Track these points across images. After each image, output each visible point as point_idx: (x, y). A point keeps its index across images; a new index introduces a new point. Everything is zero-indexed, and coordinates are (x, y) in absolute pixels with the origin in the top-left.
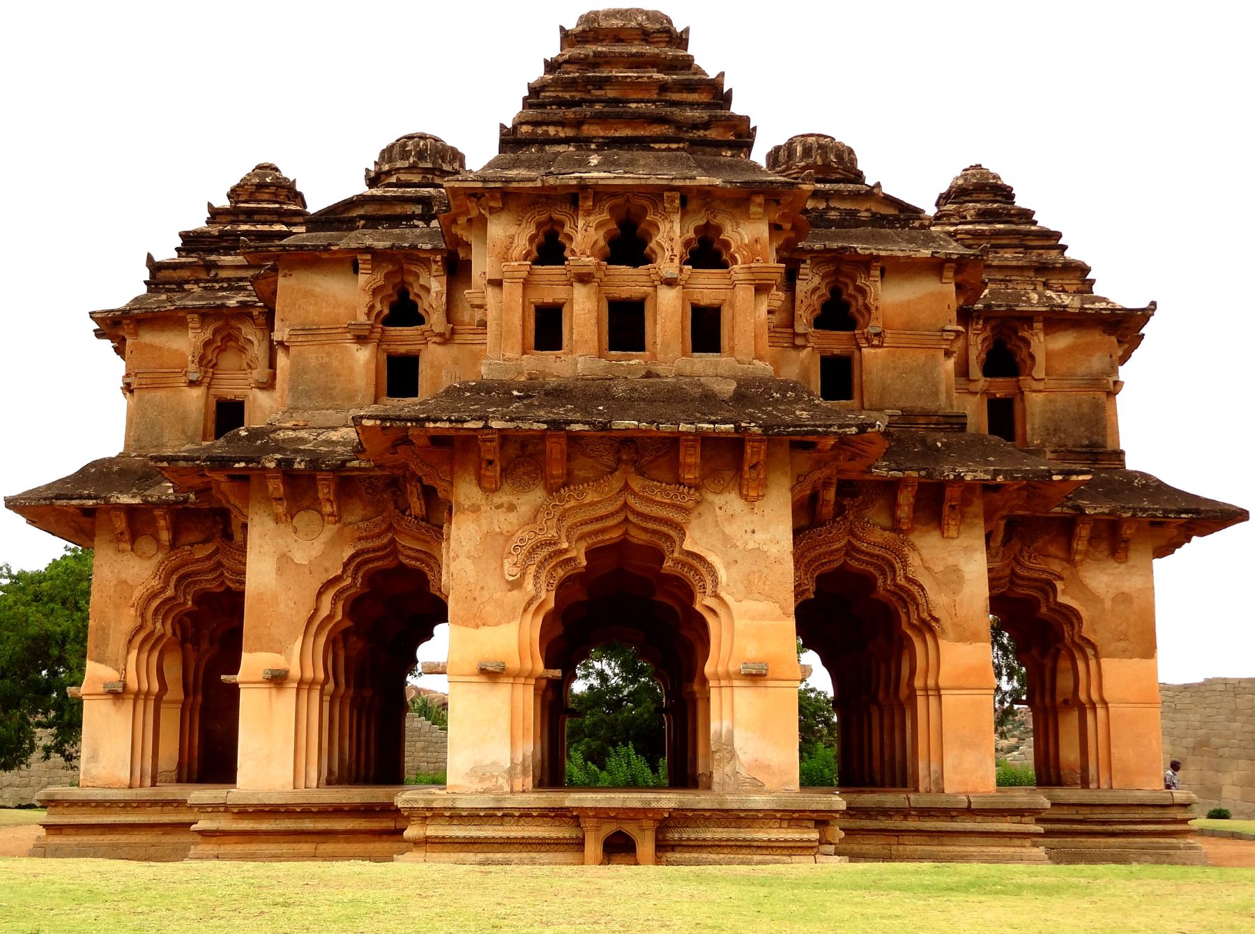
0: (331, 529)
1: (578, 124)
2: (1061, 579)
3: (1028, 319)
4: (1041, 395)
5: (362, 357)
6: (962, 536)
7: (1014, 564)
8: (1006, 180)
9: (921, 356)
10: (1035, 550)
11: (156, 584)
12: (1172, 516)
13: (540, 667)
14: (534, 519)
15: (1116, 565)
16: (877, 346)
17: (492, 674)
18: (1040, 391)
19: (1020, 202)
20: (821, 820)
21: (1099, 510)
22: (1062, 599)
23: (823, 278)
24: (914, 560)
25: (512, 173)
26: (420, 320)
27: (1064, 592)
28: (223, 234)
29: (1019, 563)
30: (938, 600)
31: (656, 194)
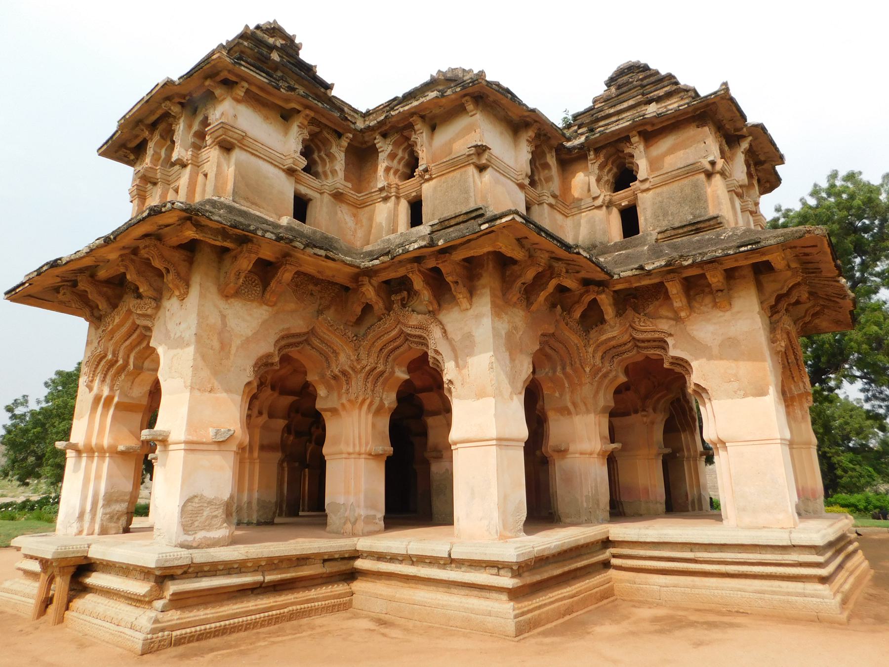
2: (670, 335)
3: (623, 138)
4: (651, 192)
6: (474, 307)
7: (631, 330)
8: (643, 61)
9: (457, 174)
10: (645, 315)
12: (731, 252)
15: (721, 314)
16: (431, 179)
18: (648, 190)
21: (657, 264)
22: (673, 352)
23: (396, 144)
27: (674, 346)
29: (634, 329)
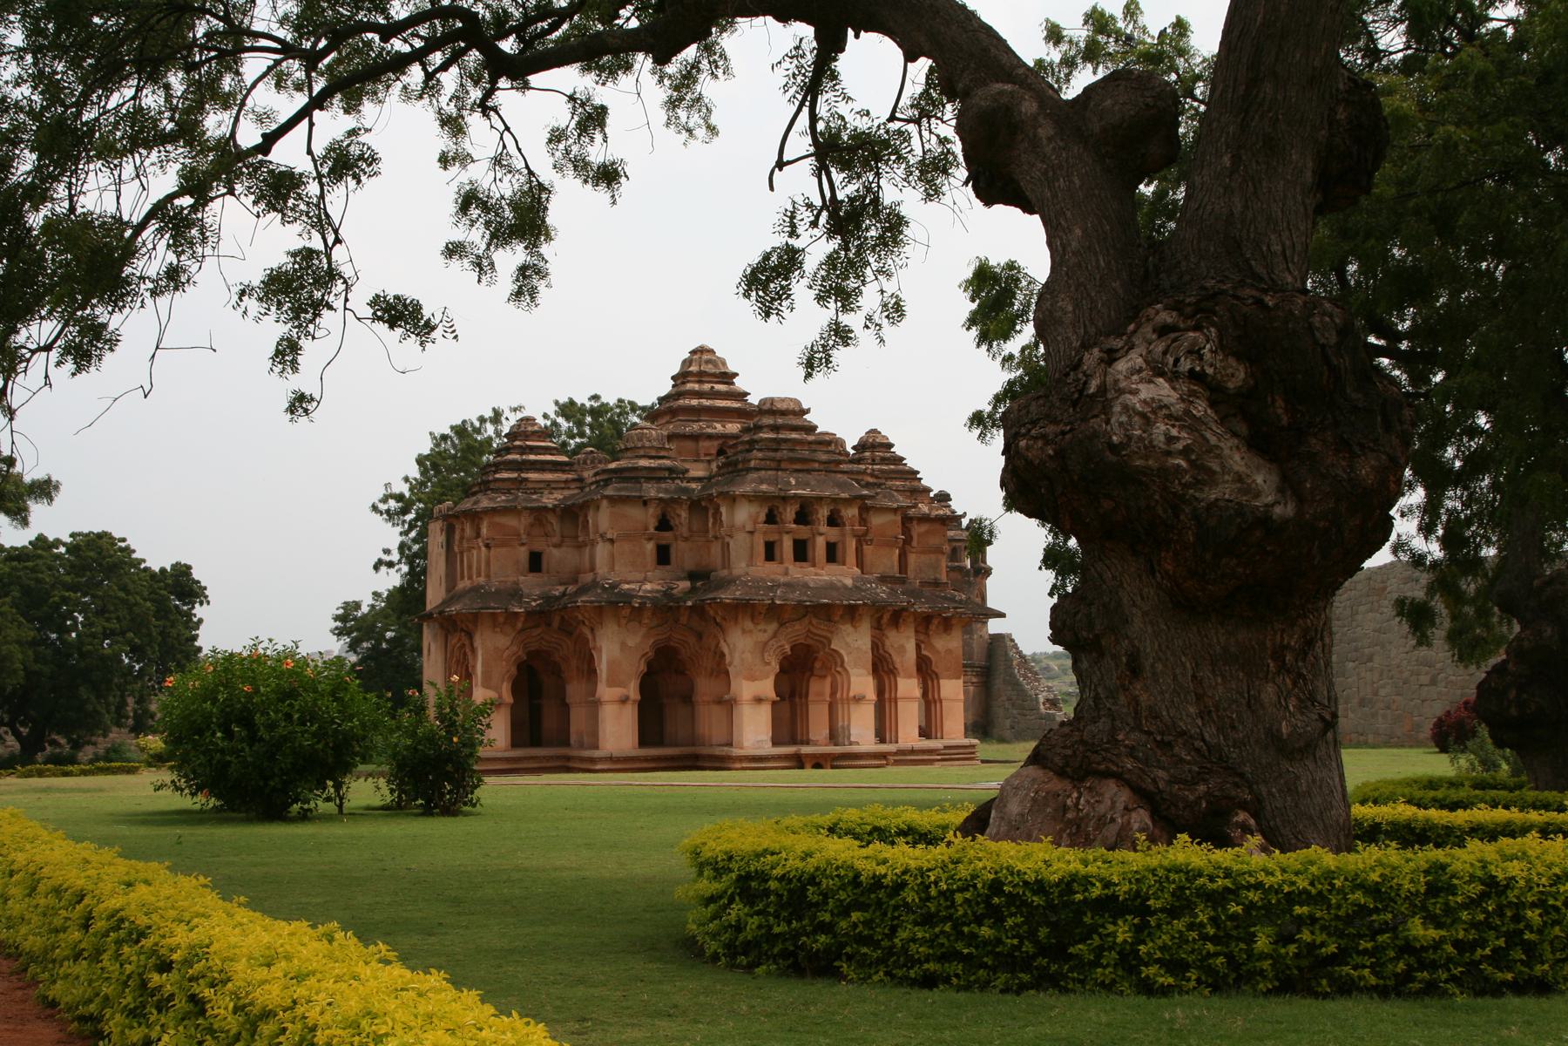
0: (644, 630)
1: (779, 461)
5: (650, 547)
8: (891, 440)
11: (515, 648)
13: (772, 695)
14: (775, 636)
17: (759, 700)
19: (898, 450)
20: (883, 756)
24: (887, 643)
25: (764, 487)
26: (670, 528)
28: (524, 462)
30: (897, 659)
31: (820, 499)
